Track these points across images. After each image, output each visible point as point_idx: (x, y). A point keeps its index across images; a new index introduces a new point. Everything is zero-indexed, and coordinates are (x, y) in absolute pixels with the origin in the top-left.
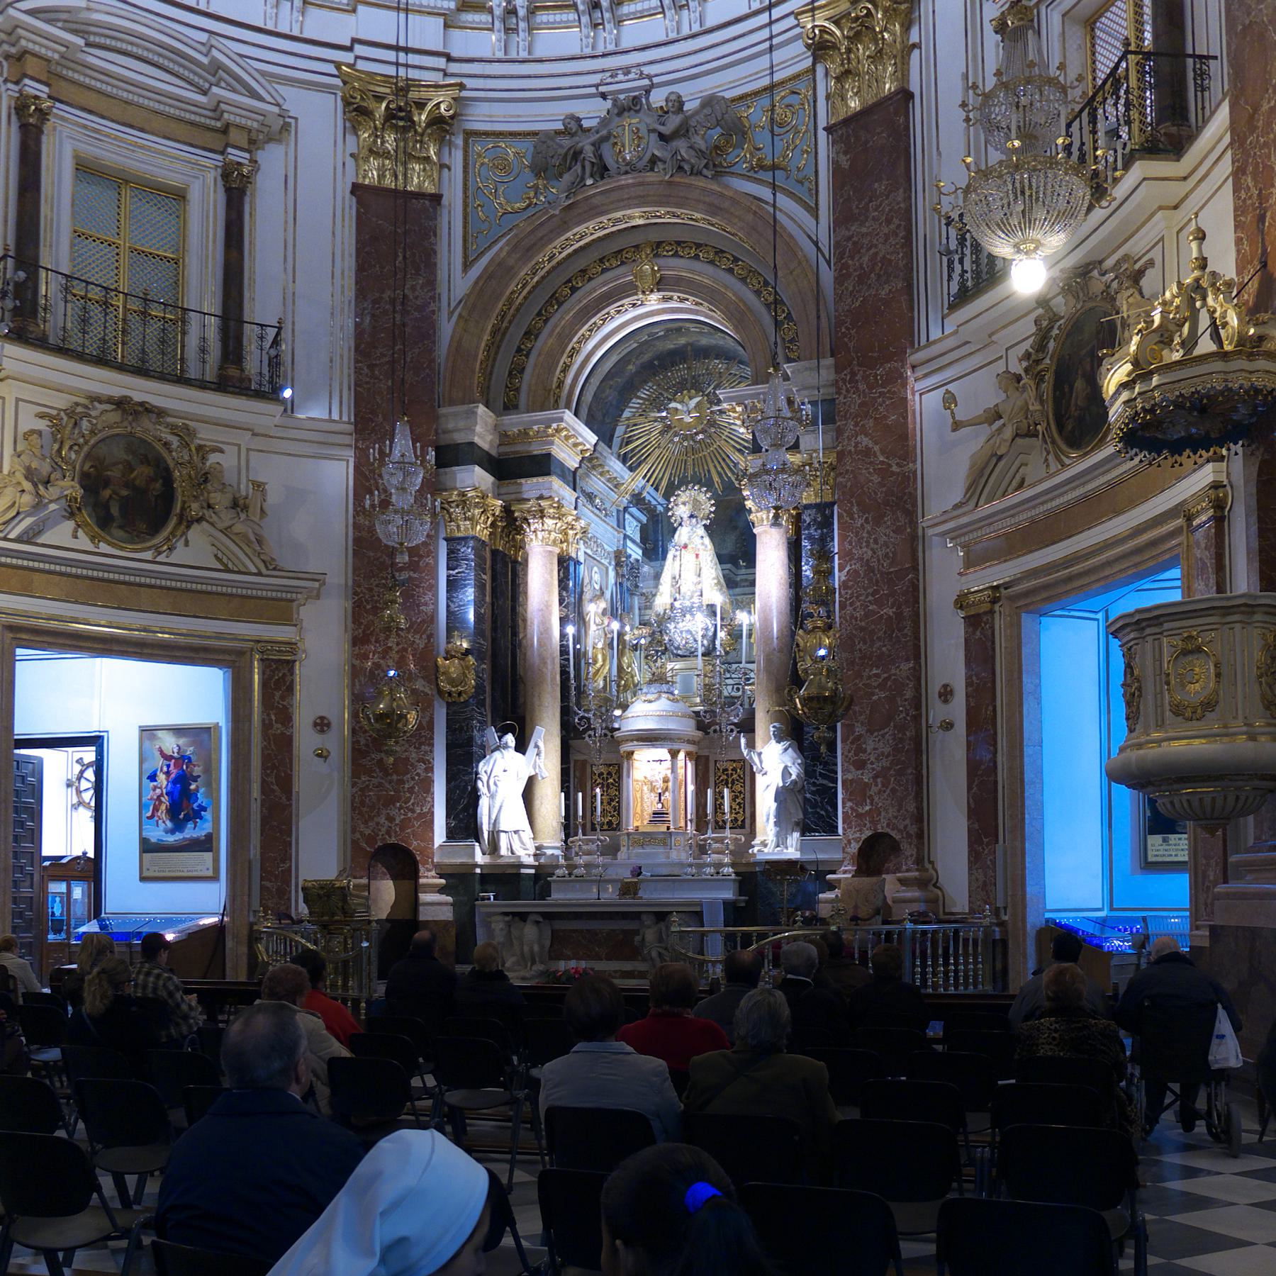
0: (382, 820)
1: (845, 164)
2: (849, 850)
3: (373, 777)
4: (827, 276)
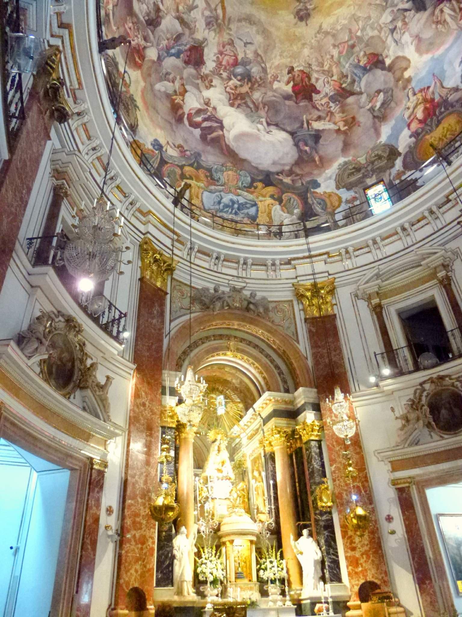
0: (132, 571)
1: (314, 330)
4: (310, 362)
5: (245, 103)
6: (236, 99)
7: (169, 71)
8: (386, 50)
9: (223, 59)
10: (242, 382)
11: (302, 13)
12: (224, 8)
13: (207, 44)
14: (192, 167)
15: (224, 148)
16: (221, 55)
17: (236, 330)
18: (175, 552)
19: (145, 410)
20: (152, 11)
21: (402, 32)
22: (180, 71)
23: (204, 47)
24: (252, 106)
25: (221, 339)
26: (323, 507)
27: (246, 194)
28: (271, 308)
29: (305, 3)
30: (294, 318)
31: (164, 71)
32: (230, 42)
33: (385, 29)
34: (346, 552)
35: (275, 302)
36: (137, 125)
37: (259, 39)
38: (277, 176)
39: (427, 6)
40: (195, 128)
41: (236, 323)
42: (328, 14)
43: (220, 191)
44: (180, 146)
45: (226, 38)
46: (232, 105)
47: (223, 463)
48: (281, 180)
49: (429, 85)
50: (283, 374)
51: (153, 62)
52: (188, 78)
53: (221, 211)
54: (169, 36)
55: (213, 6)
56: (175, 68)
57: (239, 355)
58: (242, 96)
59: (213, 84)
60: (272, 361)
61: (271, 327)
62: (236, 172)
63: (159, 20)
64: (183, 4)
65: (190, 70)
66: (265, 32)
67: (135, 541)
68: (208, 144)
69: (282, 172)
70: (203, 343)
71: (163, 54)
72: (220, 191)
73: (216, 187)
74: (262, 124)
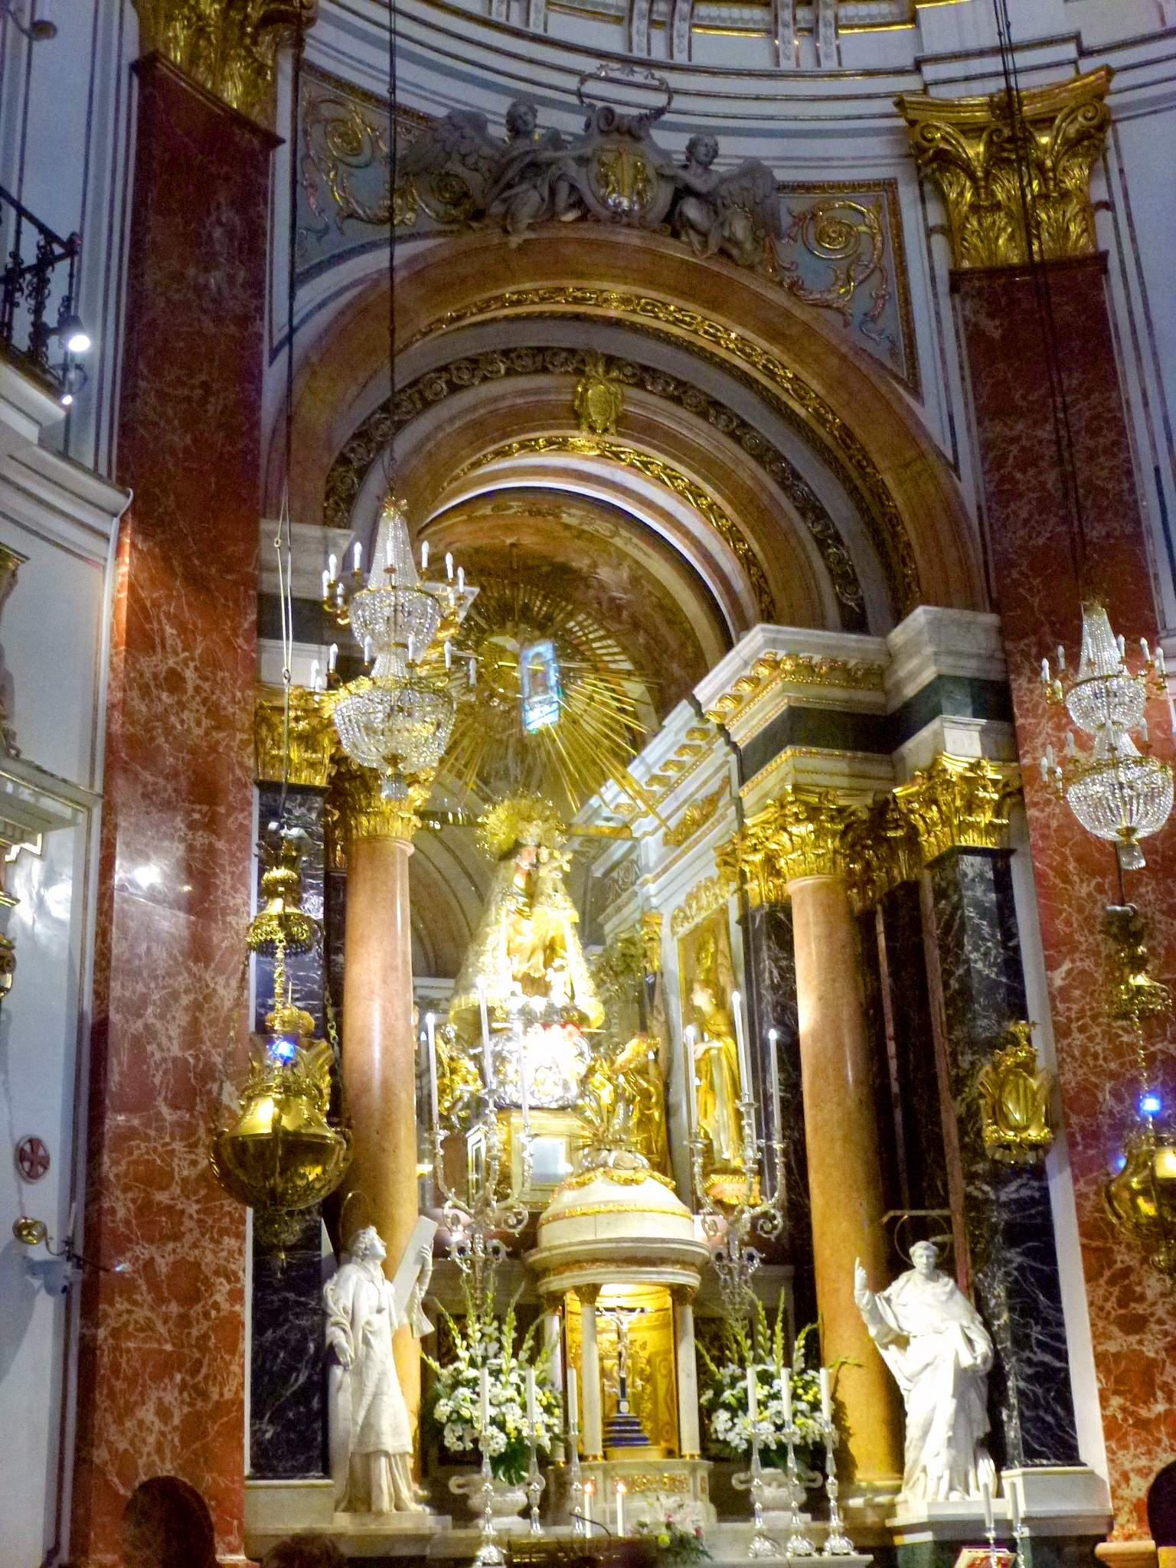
0: (147, 1413)
2: (1125, 1492)
3: (135, 1303)
4: (969, 487)
10: (640, 577)
17: (617, 323)
18: (336, 1335)
19: (182, 705)
25: (544, 370)
26: (1007, 1147)
28: (786, 221)
30: (902, 269)
34: (1098, 1336)
35: (807, 187)
41: (616, 291)
47: (551, 950)
50: (838, 539)
57: (629, 447)
60: (789, 479)
61: (787, 315)
67: (154, 1286)
70: (454, 388)
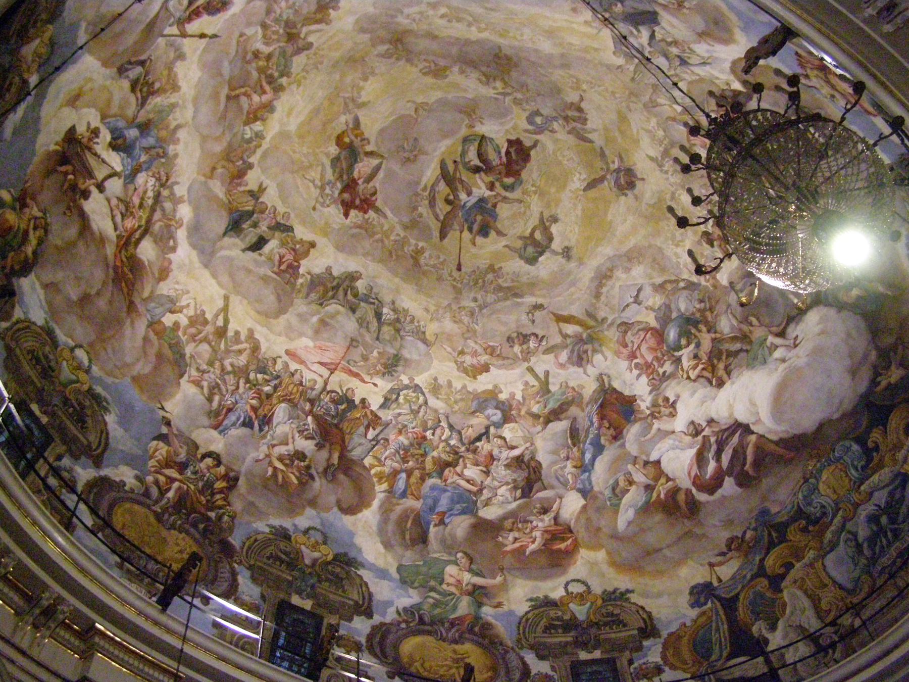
5: (730, 354)
6: (714, 369)
7: (611, 482)
8: (717, 81)
9: (643, 356)
11: (622, 181)
12: (569, 320)
13: (609, 377)
14: (775, 545)
15: (779, 450)
16: (636, 358)
20: (515, 476)
21: (688, 51)
22: (625, 458)
23: (609, 384)
24: (738, 346)
27: (875, 478)
29: (608, 169)
31: (608, 493)
32: (623, 328)
33: (678, 71)
36: (649, 615)
37: (639, 273)
38: (879, 389)
39: (649, 8)
40: (720, 485)
42: (637, 142)
43: (843, 527)
44: (731, 541)
45: (612, 334)
46: (721, 384)
48: (890, 384)
49: (793, 54)
51: (584, 507)
52: (641, 446)
53: (873, 560)
54: (563, 455)
55: (558, 340)
56: (616, 465)
58: (716, 354)
59: (671, 400)
62: (830, 462)
63: (533, 464)
64: (532, 402)
65: (633, 432)
66: (631, 257)
68: (758, 479)
69: (877, 374)
71: (583, 482)
72: (844, 526)
73: (833, 528)
74: (777, 347)
